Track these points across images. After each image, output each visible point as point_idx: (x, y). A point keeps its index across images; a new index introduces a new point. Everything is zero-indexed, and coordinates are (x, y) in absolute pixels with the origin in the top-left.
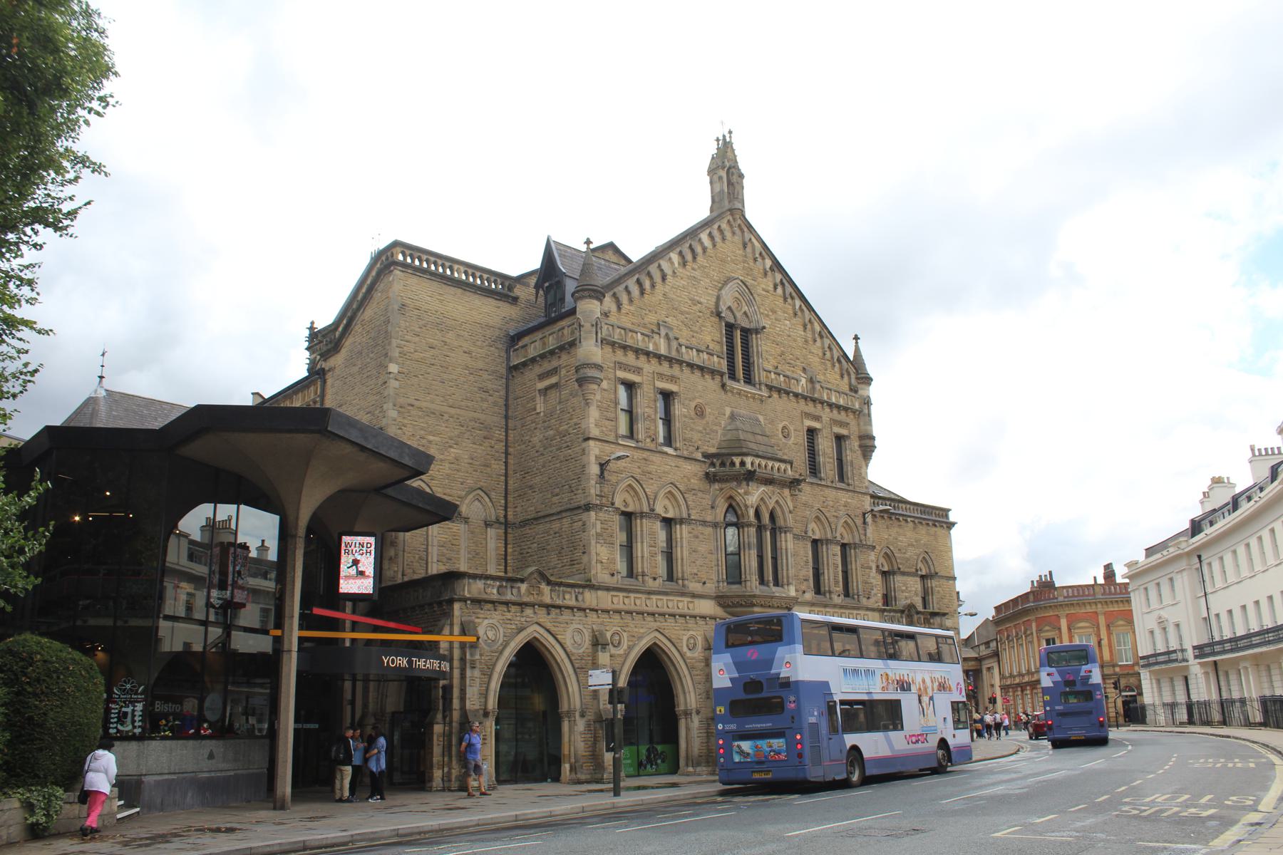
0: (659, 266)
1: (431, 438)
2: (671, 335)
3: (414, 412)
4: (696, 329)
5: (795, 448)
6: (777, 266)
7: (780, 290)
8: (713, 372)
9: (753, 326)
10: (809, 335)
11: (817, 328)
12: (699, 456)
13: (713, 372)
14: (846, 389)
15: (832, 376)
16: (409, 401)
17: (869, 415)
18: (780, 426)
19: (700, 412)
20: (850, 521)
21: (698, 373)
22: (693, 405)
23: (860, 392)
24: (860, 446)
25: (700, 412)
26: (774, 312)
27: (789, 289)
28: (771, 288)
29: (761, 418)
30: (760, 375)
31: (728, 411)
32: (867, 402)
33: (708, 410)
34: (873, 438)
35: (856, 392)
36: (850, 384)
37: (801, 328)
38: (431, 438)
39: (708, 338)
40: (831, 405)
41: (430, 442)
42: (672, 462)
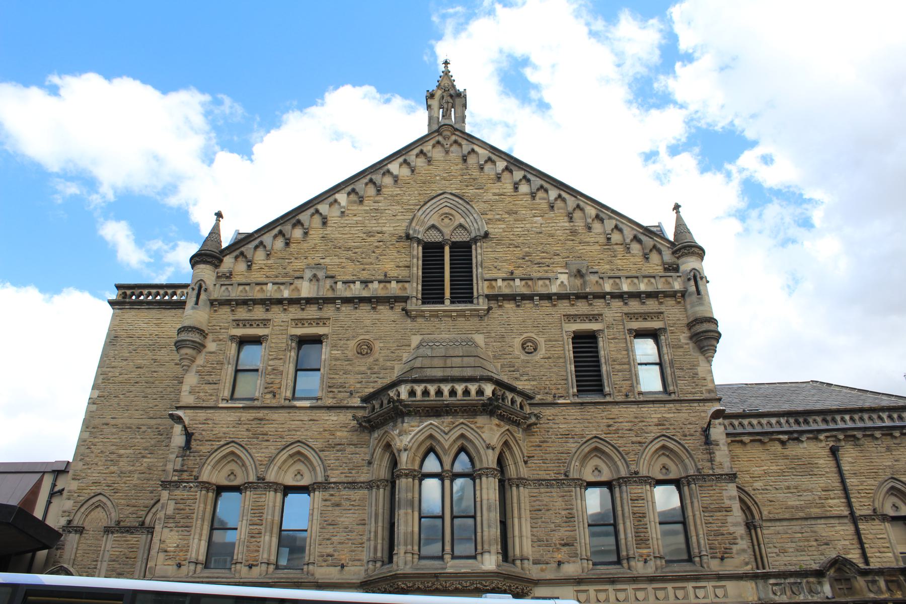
0: (317, 211)
1: (122, 452)
2: (321, 274)
3: (107, 430)
4: (372, 260)
5: (553, 367)
6: (514, 163)
7: (524, 188)
8: (390, 301)
9: (473, 235)
10: (579, 223)
11: (591, 211)
12: (356, 402)
13: (390, 301)
14: (659, 270)
15: (632, 261)
16: (104, 421)
17: (698, 292)
18: (517, 342)
19: (365, 349)
20: (671, 445)
21: (365, 307)
22: (352, 344)
23: (682, 268)
24: (691, 338)
25: (365, 349)
26: (510, 213)
27: (537, 182)
28: (509, 188)
29: (479, 339)
30: (481, 288)
31: (415, 340)
32: (697, 278)
33: (378, 345)
34: (713, 321)
35: (677, 270)
36: (664, 263)
37: (566, 219)
38: (122, 452)
39: (391, 265)
40: (620, 296)
41: (120, 456)
42: (305, 416)
